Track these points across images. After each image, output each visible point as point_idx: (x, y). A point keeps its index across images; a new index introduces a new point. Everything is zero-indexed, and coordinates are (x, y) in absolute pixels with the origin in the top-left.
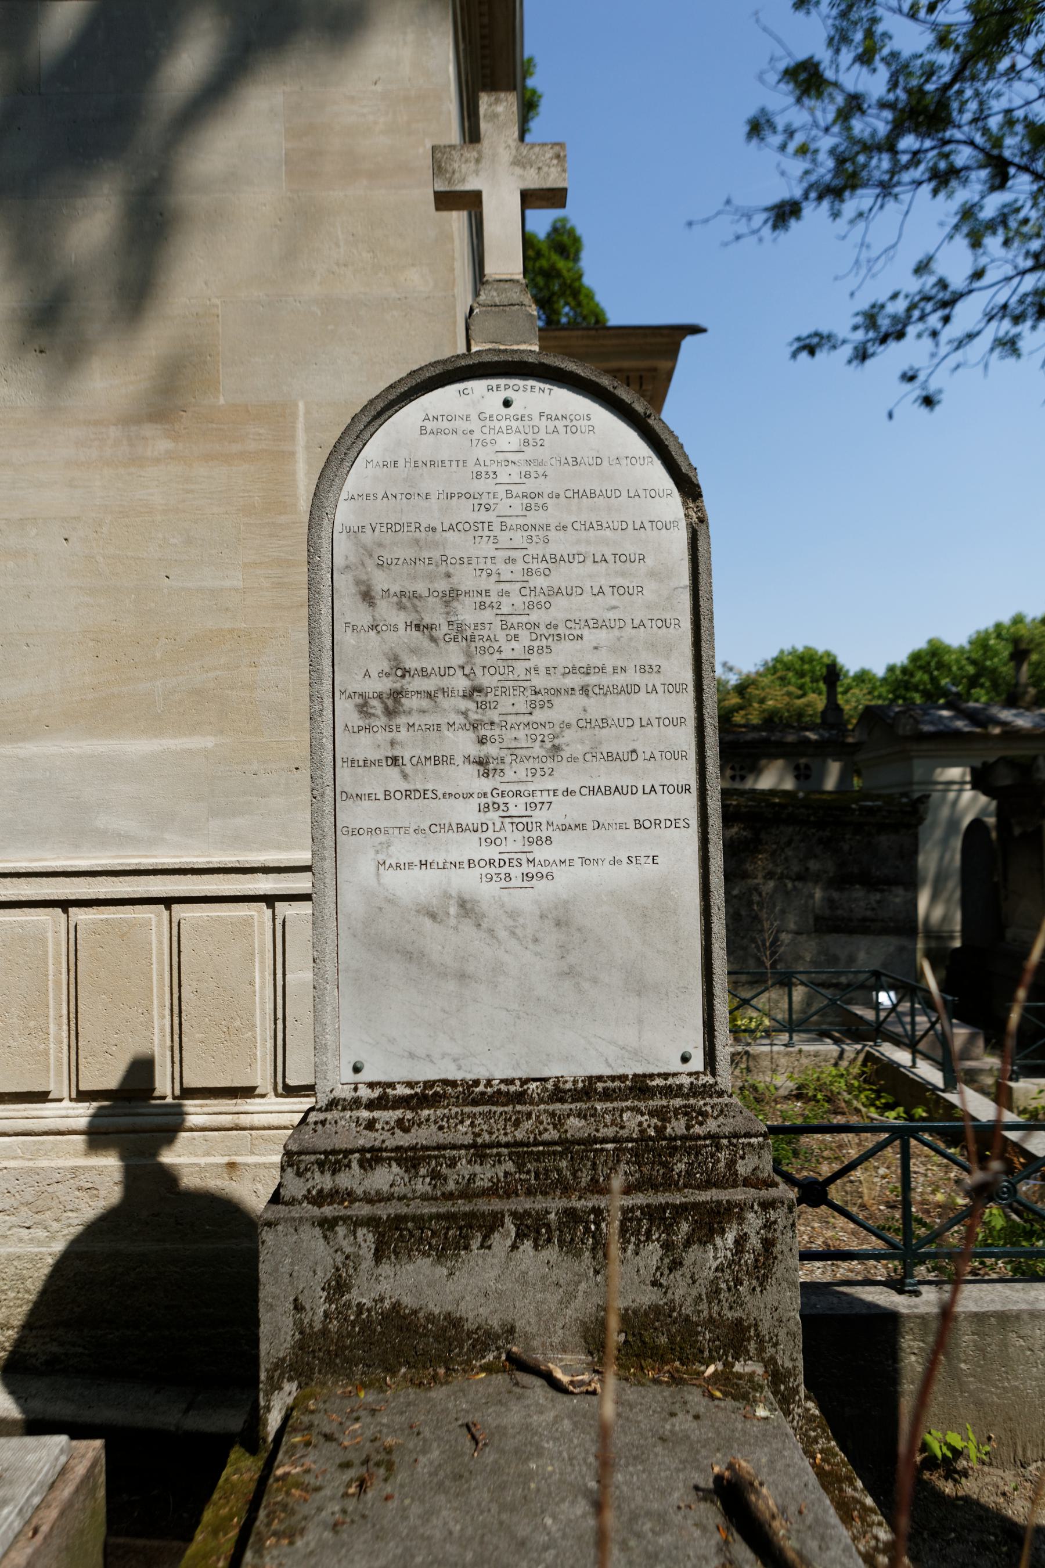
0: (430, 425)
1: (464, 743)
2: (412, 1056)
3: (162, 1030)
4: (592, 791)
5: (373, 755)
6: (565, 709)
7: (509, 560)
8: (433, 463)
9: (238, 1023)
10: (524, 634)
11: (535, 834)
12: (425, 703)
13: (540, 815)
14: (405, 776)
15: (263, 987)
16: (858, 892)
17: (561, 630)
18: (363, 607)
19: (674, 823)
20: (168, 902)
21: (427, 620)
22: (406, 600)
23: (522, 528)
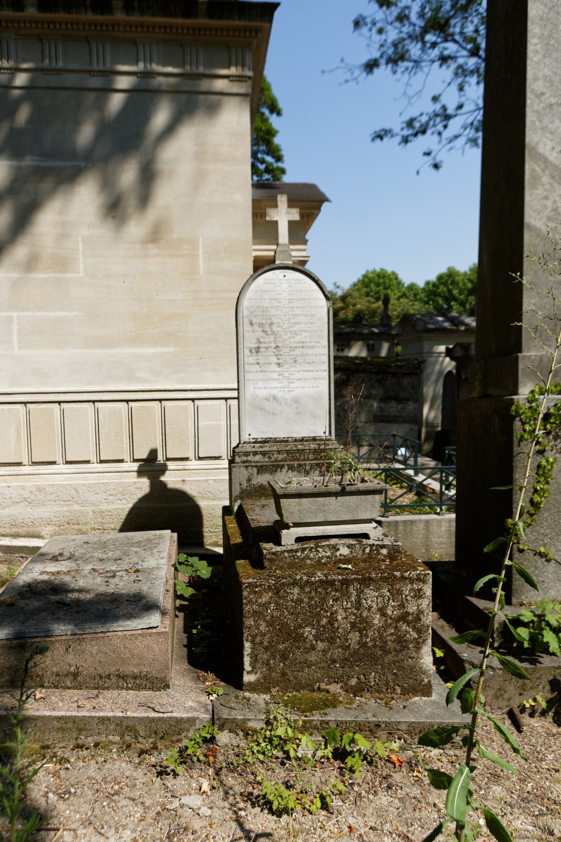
0: (266, 281)
1: (274, 359)
2: (262, 432)
3: (159, 440)
4: (304, 371)
5: (253, 362)
6: (298, 352)
7: (285, 315)
8: (267, 291)
9: (184, 438)
10: (288, 334)
11: (291, 381)
12: (265, 350)
13: (292, 377)
14: (261, 367)
15: (191, 427)
16: (393, 404)
17: (297, 333)
18: (250, 326)
19: (323, 378)
20: (160, 400)
21: (266, 330)
22: (261, 325)
23: (288, 307)
